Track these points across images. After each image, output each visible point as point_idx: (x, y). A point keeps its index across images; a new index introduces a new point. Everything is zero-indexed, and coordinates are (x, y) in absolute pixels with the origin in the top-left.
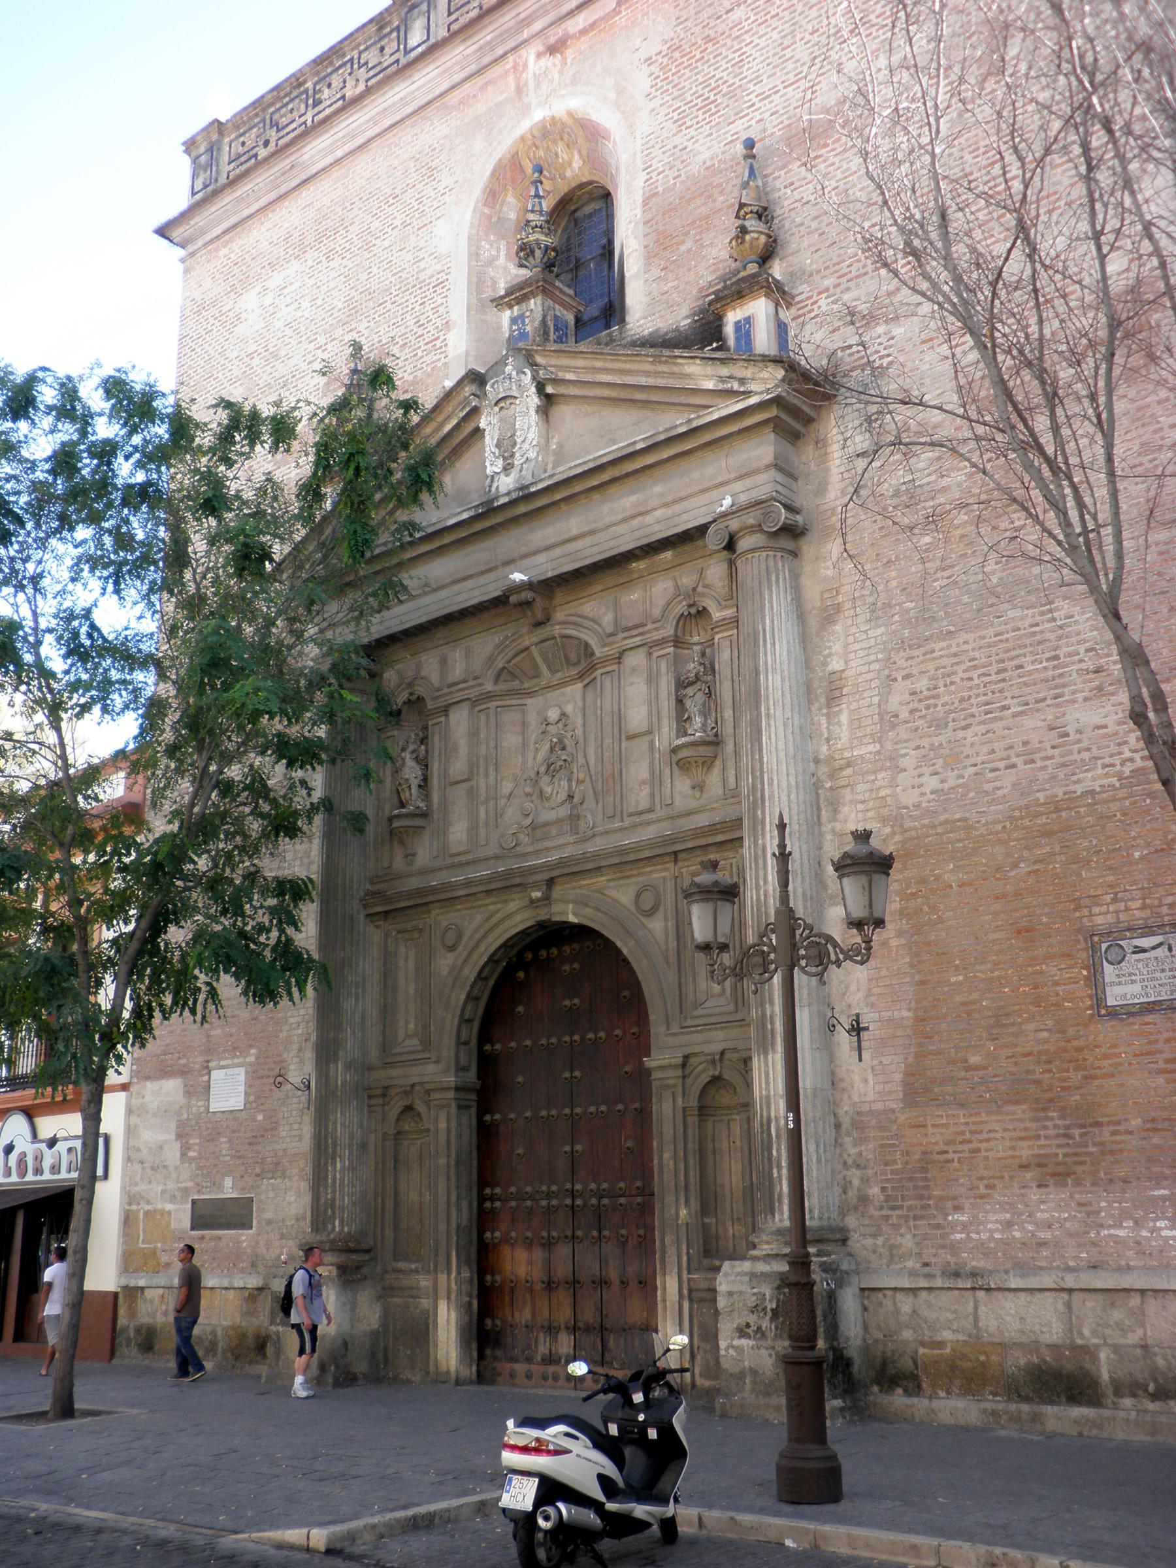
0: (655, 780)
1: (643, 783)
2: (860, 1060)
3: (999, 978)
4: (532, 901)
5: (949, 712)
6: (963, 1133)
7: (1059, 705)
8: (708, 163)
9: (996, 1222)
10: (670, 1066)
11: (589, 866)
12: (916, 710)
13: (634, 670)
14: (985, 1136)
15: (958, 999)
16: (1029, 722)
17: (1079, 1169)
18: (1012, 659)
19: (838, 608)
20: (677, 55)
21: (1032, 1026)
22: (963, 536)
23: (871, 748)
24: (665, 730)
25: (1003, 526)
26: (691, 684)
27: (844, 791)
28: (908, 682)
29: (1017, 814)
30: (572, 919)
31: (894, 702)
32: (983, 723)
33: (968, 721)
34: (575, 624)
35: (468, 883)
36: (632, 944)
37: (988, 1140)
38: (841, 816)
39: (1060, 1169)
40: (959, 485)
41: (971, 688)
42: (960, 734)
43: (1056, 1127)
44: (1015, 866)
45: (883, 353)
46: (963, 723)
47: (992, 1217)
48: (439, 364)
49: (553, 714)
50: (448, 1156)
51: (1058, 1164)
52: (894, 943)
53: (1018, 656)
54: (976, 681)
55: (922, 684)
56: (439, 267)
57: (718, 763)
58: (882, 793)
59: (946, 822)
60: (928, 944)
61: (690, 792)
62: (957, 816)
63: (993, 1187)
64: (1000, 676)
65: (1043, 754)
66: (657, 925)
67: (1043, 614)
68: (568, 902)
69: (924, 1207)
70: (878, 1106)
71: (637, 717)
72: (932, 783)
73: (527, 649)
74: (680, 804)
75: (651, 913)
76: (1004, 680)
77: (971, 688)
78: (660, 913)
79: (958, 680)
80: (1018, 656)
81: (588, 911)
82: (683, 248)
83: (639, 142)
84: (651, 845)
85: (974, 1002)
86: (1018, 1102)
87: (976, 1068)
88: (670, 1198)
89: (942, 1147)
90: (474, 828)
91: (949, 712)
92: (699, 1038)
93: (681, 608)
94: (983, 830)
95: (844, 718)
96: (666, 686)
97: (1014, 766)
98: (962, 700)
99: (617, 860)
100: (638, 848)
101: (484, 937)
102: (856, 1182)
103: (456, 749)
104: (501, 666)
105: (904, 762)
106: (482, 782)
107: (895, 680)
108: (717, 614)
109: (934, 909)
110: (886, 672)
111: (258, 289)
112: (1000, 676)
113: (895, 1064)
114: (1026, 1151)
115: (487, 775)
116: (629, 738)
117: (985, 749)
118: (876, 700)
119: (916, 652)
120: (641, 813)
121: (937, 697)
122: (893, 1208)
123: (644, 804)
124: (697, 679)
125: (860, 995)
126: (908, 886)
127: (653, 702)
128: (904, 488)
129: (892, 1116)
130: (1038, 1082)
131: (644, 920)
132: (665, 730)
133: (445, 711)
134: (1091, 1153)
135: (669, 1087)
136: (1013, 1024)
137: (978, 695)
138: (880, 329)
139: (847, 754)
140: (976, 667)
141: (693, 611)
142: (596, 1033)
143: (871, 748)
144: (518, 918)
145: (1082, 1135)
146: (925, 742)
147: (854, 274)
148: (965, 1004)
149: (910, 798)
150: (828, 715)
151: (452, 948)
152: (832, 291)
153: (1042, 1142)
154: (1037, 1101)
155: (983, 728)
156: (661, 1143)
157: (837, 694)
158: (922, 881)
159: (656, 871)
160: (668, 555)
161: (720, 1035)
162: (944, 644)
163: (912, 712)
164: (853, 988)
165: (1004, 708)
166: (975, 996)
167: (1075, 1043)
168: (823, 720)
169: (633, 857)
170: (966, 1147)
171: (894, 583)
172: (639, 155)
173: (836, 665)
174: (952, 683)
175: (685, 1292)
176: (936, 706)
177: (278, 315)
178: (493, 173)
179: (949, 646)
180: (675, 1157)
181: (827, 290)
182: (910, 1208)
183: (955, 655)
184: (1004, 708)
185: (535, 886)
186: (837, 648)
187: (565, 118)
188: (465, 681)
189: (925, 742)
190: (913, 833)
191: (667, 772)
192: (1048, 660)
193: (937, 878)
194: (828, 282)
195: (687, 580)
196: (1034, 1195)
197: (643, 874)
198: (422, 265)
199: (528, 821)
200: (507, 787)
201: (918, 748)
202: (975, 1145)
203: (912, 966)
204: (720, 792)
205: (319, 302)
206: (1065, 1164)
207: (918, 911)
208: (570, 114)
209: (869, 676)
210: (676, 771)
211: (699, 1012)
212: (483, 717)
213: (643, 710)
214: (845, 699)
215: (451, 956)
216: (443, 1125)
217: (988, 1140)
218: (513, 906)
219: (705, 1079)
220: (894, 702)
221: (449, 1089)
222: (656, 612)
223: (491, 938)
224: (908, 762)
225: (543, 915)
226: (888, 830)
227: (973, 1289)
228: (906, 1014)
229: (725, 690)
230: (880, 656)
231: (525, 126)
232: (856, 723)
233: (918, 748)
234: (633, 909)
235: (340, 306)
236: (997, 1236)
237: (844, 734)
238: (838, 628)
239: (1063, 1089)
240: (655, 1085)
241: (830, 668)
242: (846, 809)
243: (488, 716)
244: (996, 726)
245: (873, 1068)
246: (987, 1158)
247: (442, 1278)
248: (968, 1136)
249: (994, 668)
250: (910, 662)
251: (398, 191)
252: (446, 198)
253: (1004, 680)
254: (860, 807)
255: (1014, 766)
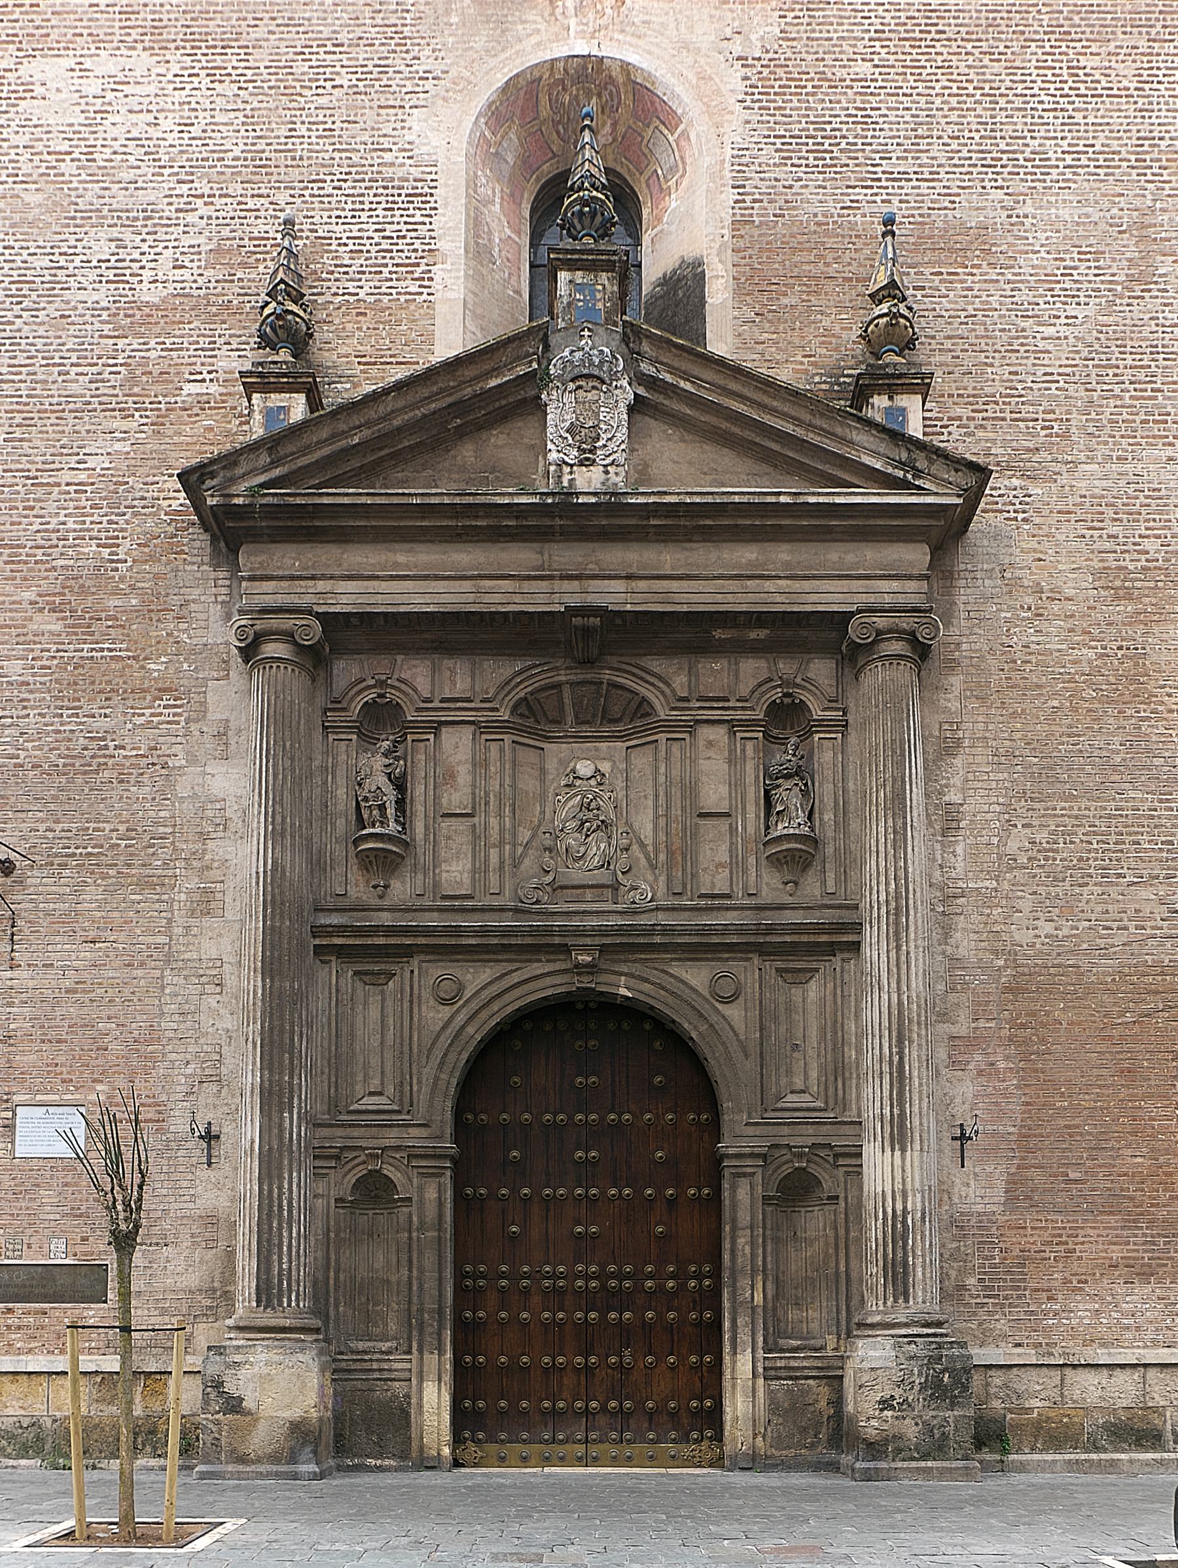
0: (736, 864)
1: (721, 865)
2: (963, 1166)
3: (1102, 1109)
4: (577, 965)
5: (1068, 868)
6: (1060, 1236)
7: (1170, 885)
8: (820, 218)
9: (1086, 1310)
10: (752, 1155)
11: (658, 940)
12: (1035, 859)
13: (710, 744)
14: (1080, 1239)
15: (1062, 1122)
16: (1146, 893)
17: (1161, 1271)
18: (1130, 834)
19: (958, 742)
20: (780, 72)
21: (1129, 1152)
22: (1089, 710)
23: (987, 883)
24: (751, 816)
25: (1129, 712)
26: (788, 777)
27: (956, 917)
28: (1028, 831)
29: (1126, 970)
30: (623, 991)
31: (1012, 846)
32: (1100, 884)
33: (1086, 880)
34: (634, 675)
35: (484, 931)
36: (704, 1028)
37: (1083, 1243)
38: (952, 941)
39: (1146, 1269)
40: (1090, 662)
41: (1089, 851)
42: (1077, 890)
43: (1145, 1235)
44: (1122, 1014)
45: (1018, 506)
46: (1081, 881)
47: (1081, 1306)
48: (419, 299)
49: (584, 768)
50: (440, 1229)
51: (1143, 1265)
52: (1002, 1065)
53: (1137, 833)
54: (1095, 846)
55: (1042, 836)
56: (416, 172)
57: (817, 863)
58: (997, 928)
59: (1059, 966)
60: (1036, 1071)
61: (781, 886)
62: (1070, 962)
63: (1086, 1282)
64: (1119, 847)
65: (1153, 923)
66: (734, 1013)
67: (1161, 801)
68: (621, 974)
69: (1019, 1297)
70: (979, 1208)
71: (714, 795)
72: (1049, 928)
73: (558, 686)
74: (767, 896)
75: (728, 1001)
76: (1122, 851)
77: (1089, 851)
78: (741, 999)
79: (1077, 840)
80: (1137, 833)
81: (646, 987)
82: (785, 301)
83: (729, 152)
84: (740, 930)
85: (1077, 1127)
86: (1111, 1213)
87: (1076, 1181)
88: (744, 1282)
89: (1039, 1247)
90: (479, 870)
91: (1068, 868)
92: (786, 1130)
93: (777, 694)
94: (1093, 978)
95: (959, 850)
96: (751, 771)
97: (1126, 928)
98: (1080, 859)
99: (695, 940)
100: (725, 930)
101: (499, 995)
102: (953, 1273)
103: (451, 776)
104: (522, 694)
105: (1020, 904)
106: (494, 822)
107: (1016, 826)
108: (817, 713)
109: (1043, 1041)
110: (1007, 817)
111: (71, 62)
112: (1119, 847)
113: (998, 1172)
114: (1116, 1253)
115: (500, 816)
116: (701, 815)
117: (1099, 908)
118: (995, 840)
119: (1037, 805)
120: (714, 896)
121: (1056, 851)
122: (989, 1297)
123: (722, 887)
124: (798, 773)
125: (967, 1106)
126: (1019, 1016)
127: (736, 784)
128: (1033, 646)
129: (994, 1218)
130: (1132, 1198)
131: (717, 1005)
132: (751, 816)
133: (437, 727)
134: (1172, 1258)
135: (745, 1175)
136: (1112, 1148)
137: (1096, 859)
138: (1015, 482)
139: (960, 884)
140: (1095, 833)
141: (787, 700)
142: (620, 1115)
143: (987, 883)
144: (548, 981)
145: (1165, 1243)
146: (1041, 889)
147: (990, 414)
148: (1066, 1126)
149: (1023, 937)
150: (943, 845)
151: (445, 1002)
152: (965, 421)
153: (1131, 1247)
154: (1129, 1213)
155: (1099, 890)
156: (734, 1228)
157: (954, 825)
158: (1033, 1014)
159: (734, 959)
160: (762, 634)
161: (811, 1130)
162: (1067, 805)
163: (1030, 859)
164: (958, 1100)
165: (1119, 876)
166: (1077, 1121)
167: (1165, 1169)
168: (938, 846)
169: (716, 940)
170: (1062, 1248)
171: (1018, 735)
172: (727, 165)
173: (953, 797)
174: (1072, 842)
175: (761, 1370)
176: (1055, 859)
177: (112, 118)
178: (505, 89)
179: (1071, 808)
180: (753, 1244)
181: (960, 418)
182: (1005, 1298)
183: (1076, 817)
184: (1119, 876)
185: (585, 949)
186: (957, 781)
187: (616, 73)
188: (469, 700)
189: (1041, 889)
190: (1026, 970)
191: (752, 860)
192: (1162, 843)
193: (1047, 1014)
194: (959, 411)
195: (786, 667)
196: (1120, 1289)
197: (719, 959)
198: (388, 157)
199: (549, 878)
200: (524, 835)
201: (1035, 893)
202: (1071, 1246)
203: (1018, 1087)
204: (817, 893)
205: (196, 131)
206: (1150, 1266)
207: (1026, 1042)
208: (626, 67)
209: (989, 816)
210: (764, 862)
211: (780, 1105)
212: (494, 747)
213: (724, 790)
214: (962, 832)
215: (446, 1012)
216: (431, 1194)
217: (1083, 1243)
218: (537, 968)
219: (786, 1170)
220: (1012, 846)
221: (444, 1157)
222: (744, 691)
223: (507, 998)
224: (1026, 904)
225: (586, 982)
226: (1001, 963)
227: (1064, 1365)
228: (1012, 1130)
229: (825, 791)
230: (1001, 800)
231: (560, 51)
232: (973, 855)
233: (1035, 893)
234: (706, 993)
235: (237, 152)
236: (1086, 1321)
237: (960, 865)
238: (958, 762)
239: (1152, 1205)
240: (726, 1172)
241: (946, 798)
242: (958, 935)
243: (502, 750)
244: (1111, 890)
245: (976, 1174)
246: (1080, 1258)
247: (431, 1359)
248: (1064, 1239)
249: (1113, 838)
250: (1030, 813)
251: (343, 37)
252: (428, 85)
253: (1122, 851)
254: (973, 936)
255: (1126, 928)
